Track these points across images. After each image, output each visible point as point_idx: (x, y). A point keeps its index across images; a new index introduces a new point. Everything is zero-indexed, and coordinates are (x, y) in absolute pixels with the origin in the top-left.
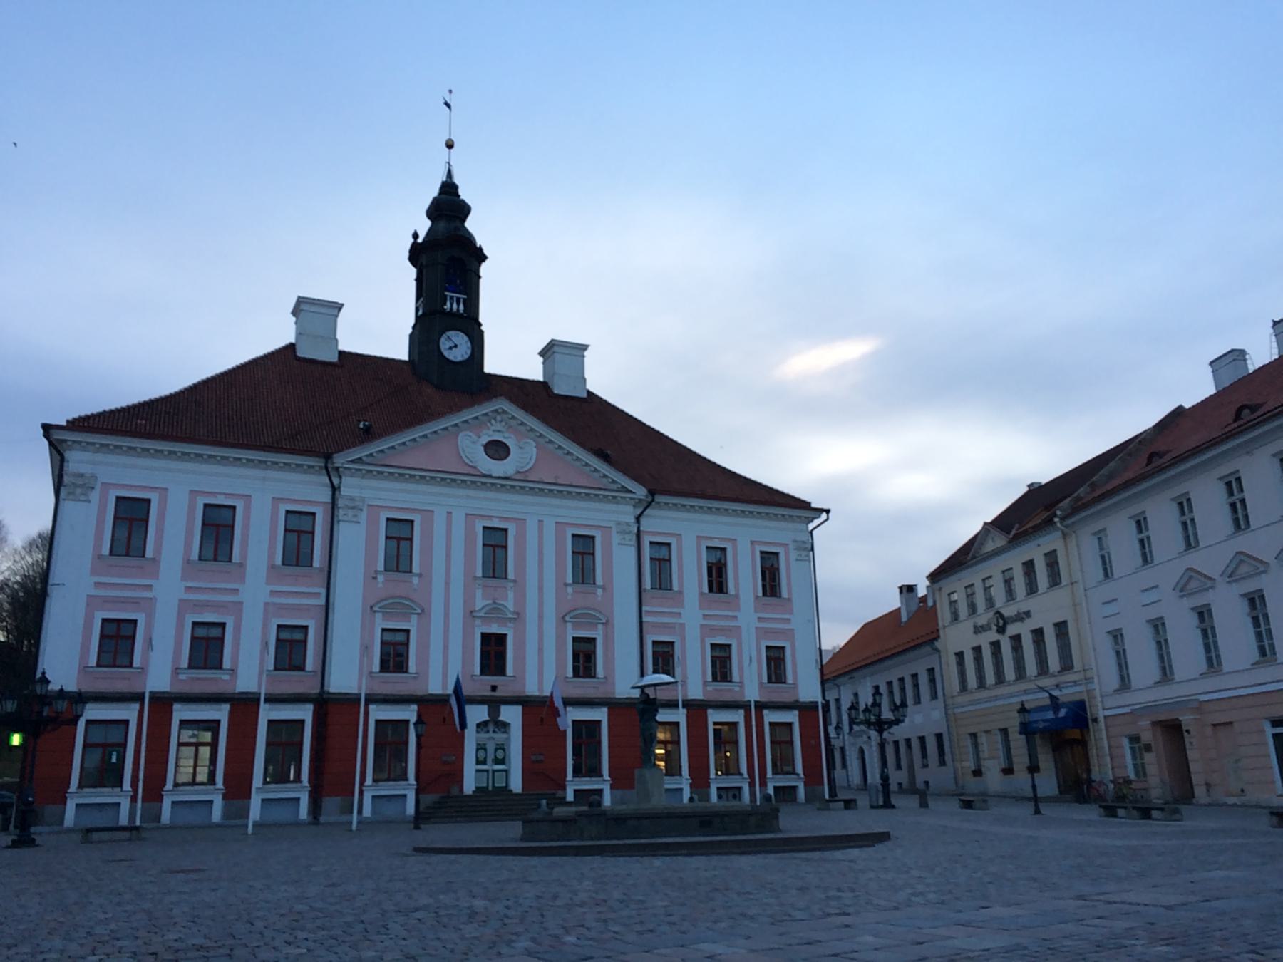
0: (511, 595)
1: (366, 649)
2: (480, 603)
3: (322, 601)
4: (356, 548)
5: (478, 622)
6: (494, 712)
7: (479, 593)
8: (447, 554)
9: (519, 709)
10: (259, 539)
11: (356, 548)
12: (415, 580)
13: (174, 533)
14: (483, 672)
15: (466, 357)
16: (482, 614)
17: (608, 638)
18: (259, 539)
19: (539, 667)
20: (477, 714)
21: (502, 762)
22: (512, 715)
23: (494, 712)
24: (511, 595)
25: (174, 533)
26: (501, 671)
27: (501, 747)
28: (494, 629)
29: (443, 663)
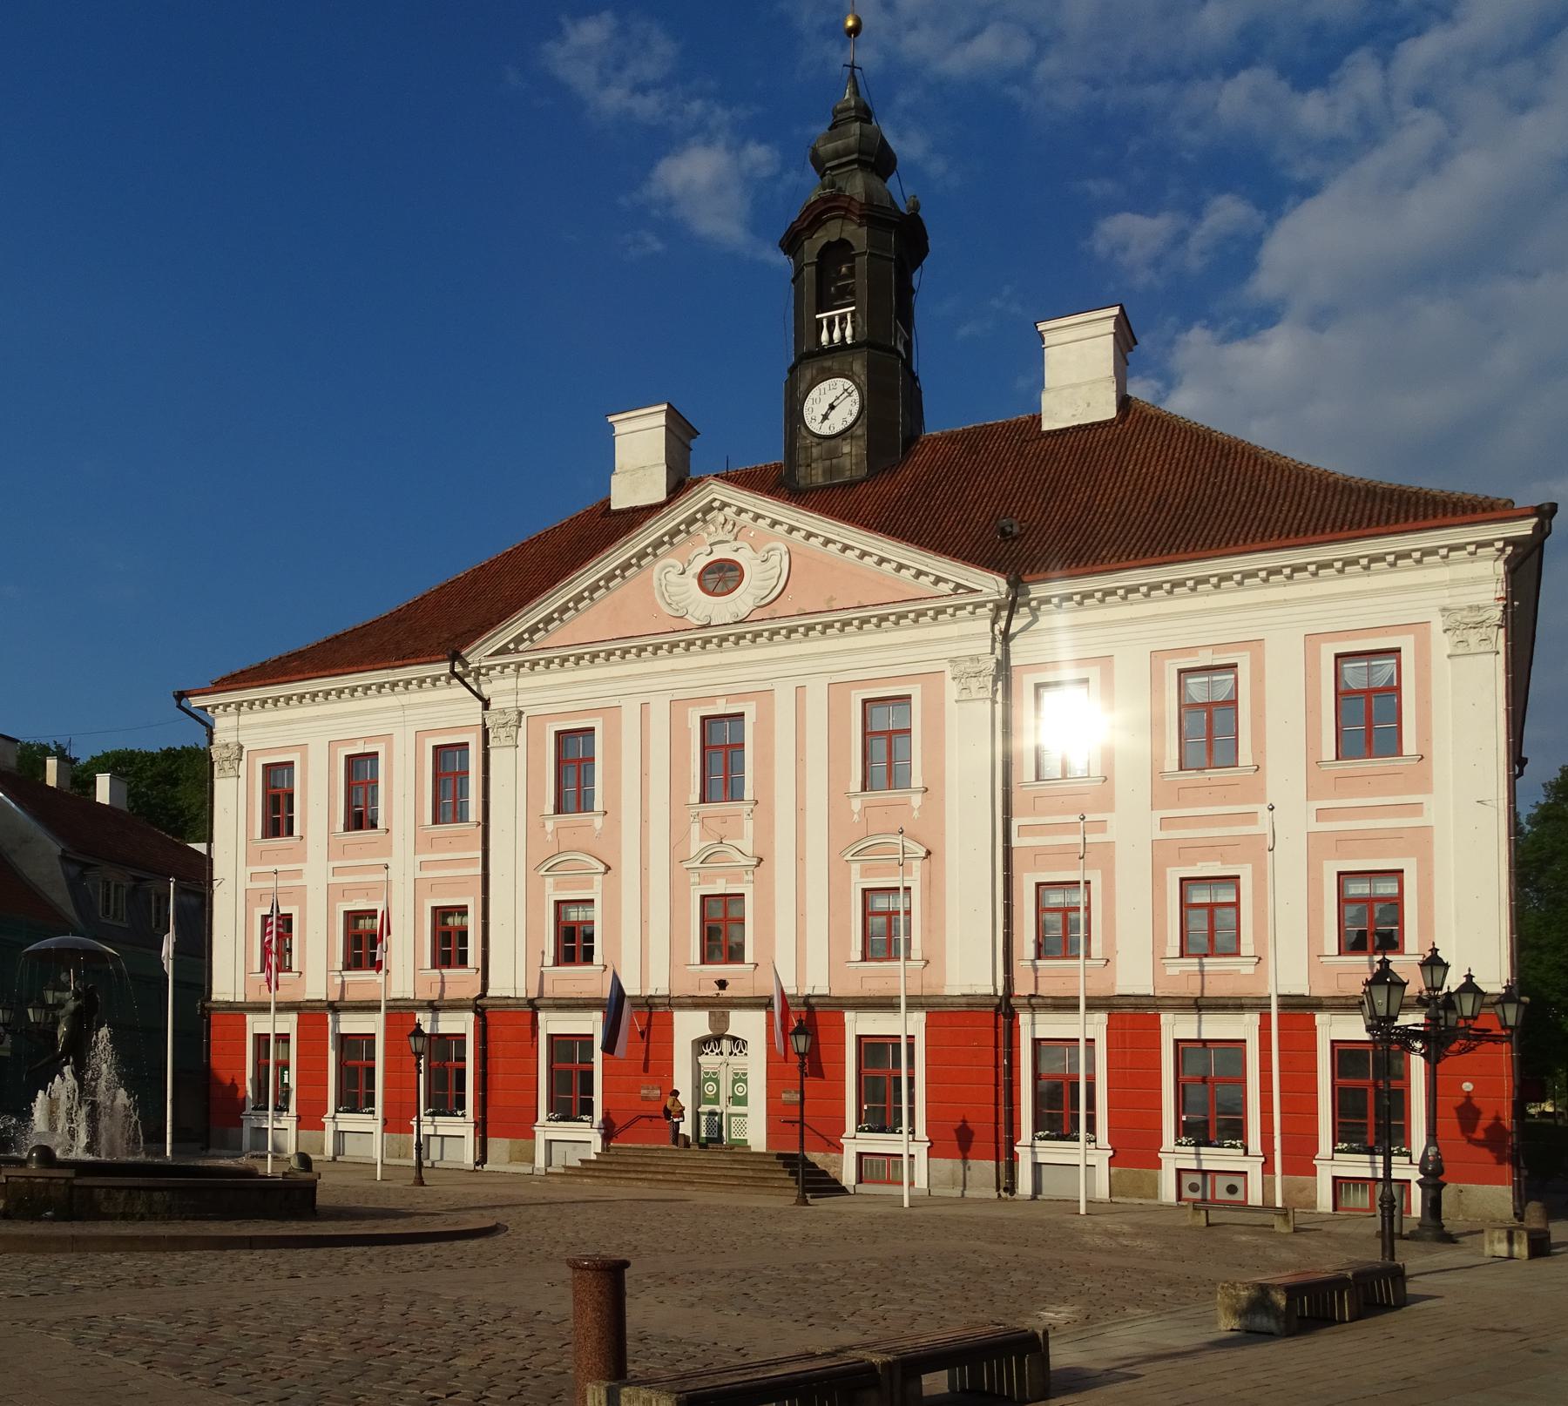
0: (749, 826)
1: (531, 931)
2: (696, 845)
3: (479, 870)
4: (516, 780)
5: (694, 879)
6: (719, 1022)
7: (696, 829)
8: (646, 771)
9: (760, 1016)
10: (404, 791)
11: (516, 780)
12: (598, 822)
13: (318, 800)
14: (704, 961)
15: (850, 420)
16: (697, 864)
17: (932, 885)
18: (404, 791)
19: (803, 948)
20: (690, 1026)
21: (742, 1101)
22: (749, 1025)
23: (719, 1022)
24: (749, 826)
25: (318, 800)
26: (735, 954)
27: (740, 1078)
28: (720, 887)
29: (647, 950)
